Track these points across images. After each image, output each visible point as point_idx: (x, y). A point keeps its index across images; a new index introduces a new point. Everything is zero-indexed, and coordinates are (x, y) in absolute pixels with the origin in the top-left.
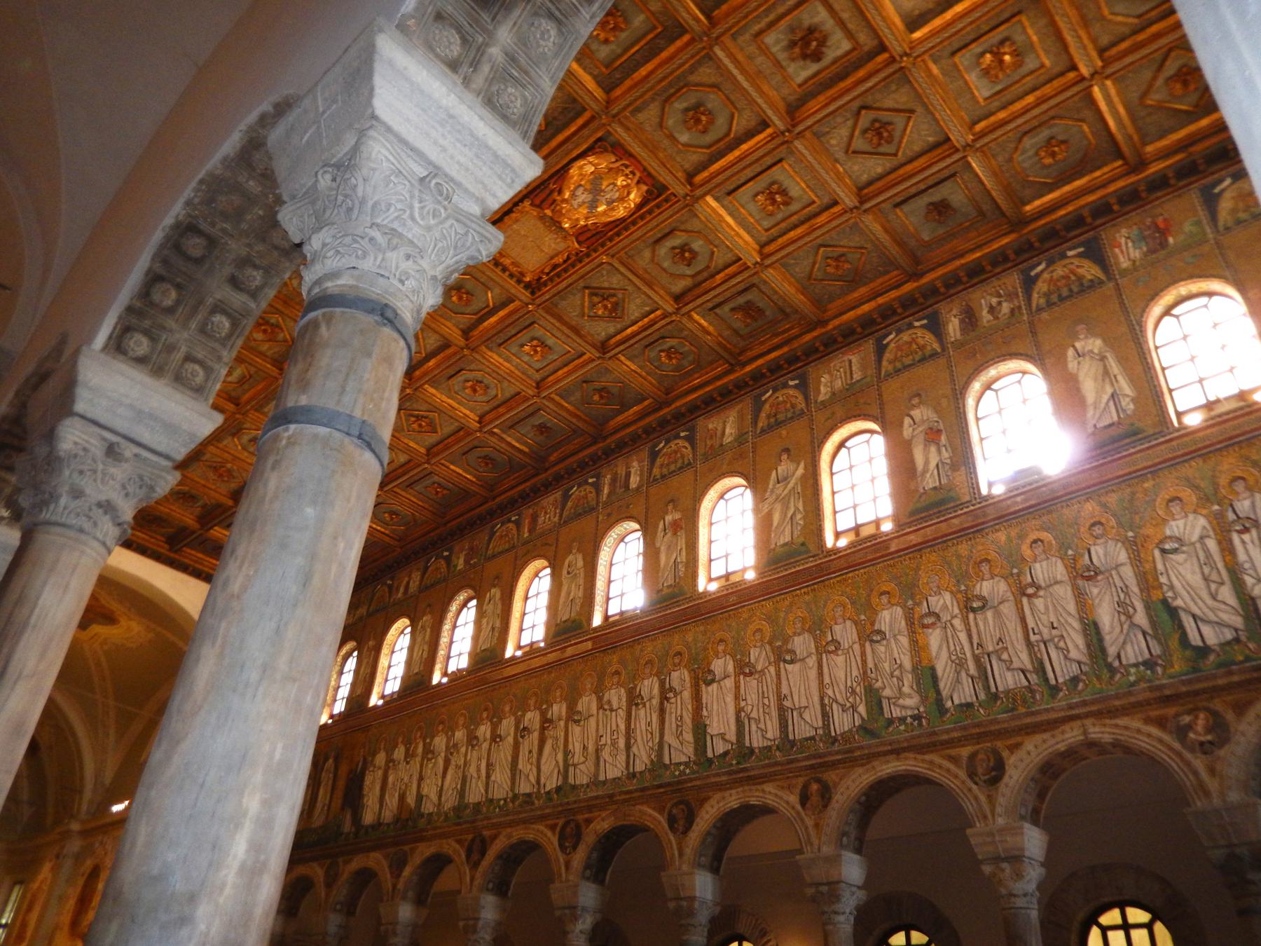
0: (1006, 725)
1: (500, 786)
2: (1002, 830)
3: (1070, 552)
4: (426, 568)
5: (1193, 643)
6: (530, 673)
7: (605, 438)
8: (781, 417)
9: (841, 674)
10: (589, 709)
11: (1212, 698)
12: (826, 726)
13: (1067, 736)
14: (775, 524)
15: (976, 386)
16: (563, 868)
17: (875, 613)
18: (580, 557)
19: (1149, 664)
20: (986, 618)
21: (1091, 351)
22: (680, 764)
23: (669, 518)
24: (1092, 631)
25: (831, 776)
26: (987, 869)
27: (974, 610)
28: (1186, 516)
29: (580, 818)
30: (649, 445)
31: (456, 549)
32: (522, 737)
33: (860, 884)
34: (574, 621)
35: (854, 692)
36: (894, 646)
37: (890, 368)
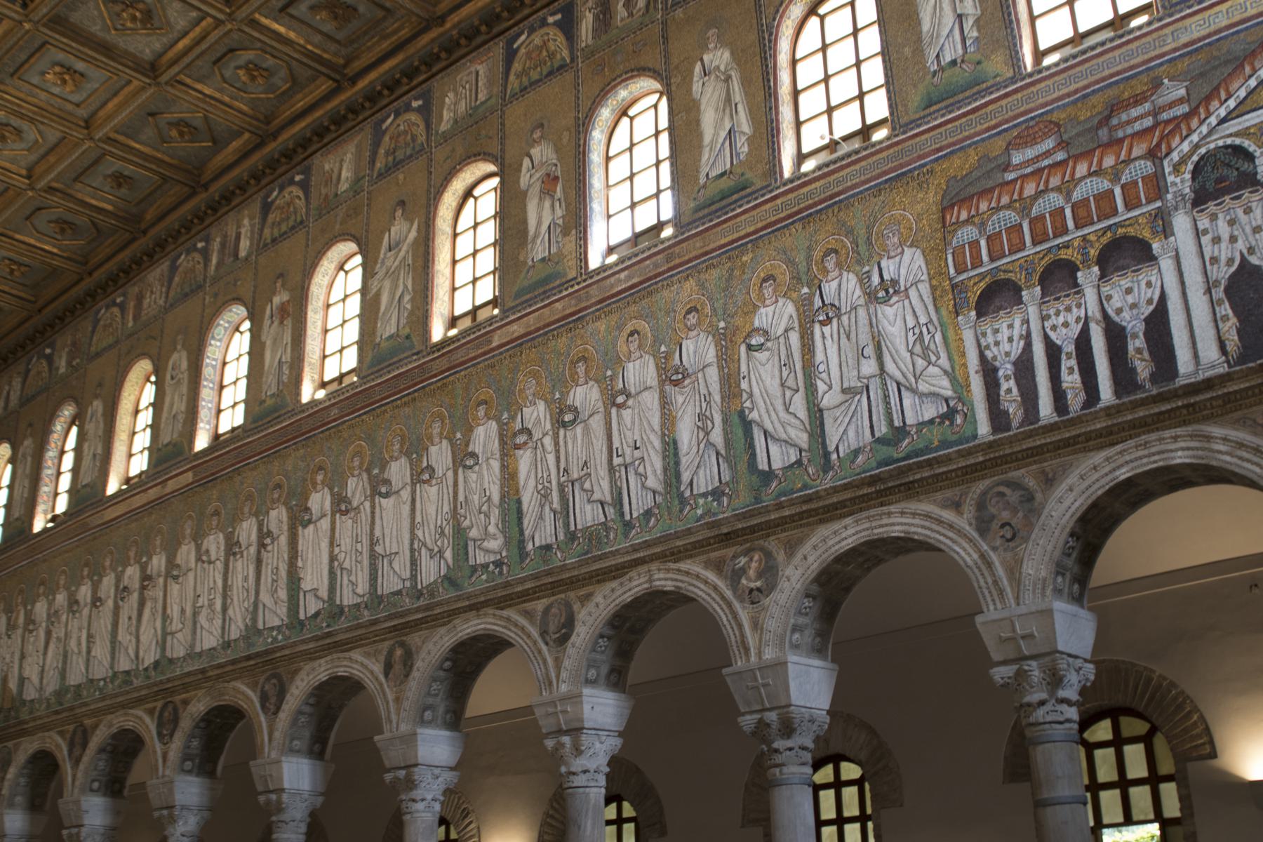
1: (100, 662)
2: (563, 699)
3: (663, 349)
4: (28, 371)
5: (760, 467)
6: (133, 515)
7: (206, 187)
8: (400, 155)
9: (431, 510)
10: (187, 562)
11: (768, 536)
12: (414, 577)
13: (635, 583)
14: (383, 308)
15: (605, 114)
16: (160, 761)
17: (470, 430)
18: (184, 354)
19: (717, 494)
21: (718, 68)
22: (272, 628)
23: (277, 300)
24: (671, 449)
25: (414, 639)
26: (550, 743)
27: (564, 425)
28: (777, 301)
29: (177, 698)
30: (262, 194)
31: (59, 344)
32: (122, 599)
33: (452, 763)
34: (175, 445)
35: (442, 533)
36: (485, 473)
37: (516, 86)
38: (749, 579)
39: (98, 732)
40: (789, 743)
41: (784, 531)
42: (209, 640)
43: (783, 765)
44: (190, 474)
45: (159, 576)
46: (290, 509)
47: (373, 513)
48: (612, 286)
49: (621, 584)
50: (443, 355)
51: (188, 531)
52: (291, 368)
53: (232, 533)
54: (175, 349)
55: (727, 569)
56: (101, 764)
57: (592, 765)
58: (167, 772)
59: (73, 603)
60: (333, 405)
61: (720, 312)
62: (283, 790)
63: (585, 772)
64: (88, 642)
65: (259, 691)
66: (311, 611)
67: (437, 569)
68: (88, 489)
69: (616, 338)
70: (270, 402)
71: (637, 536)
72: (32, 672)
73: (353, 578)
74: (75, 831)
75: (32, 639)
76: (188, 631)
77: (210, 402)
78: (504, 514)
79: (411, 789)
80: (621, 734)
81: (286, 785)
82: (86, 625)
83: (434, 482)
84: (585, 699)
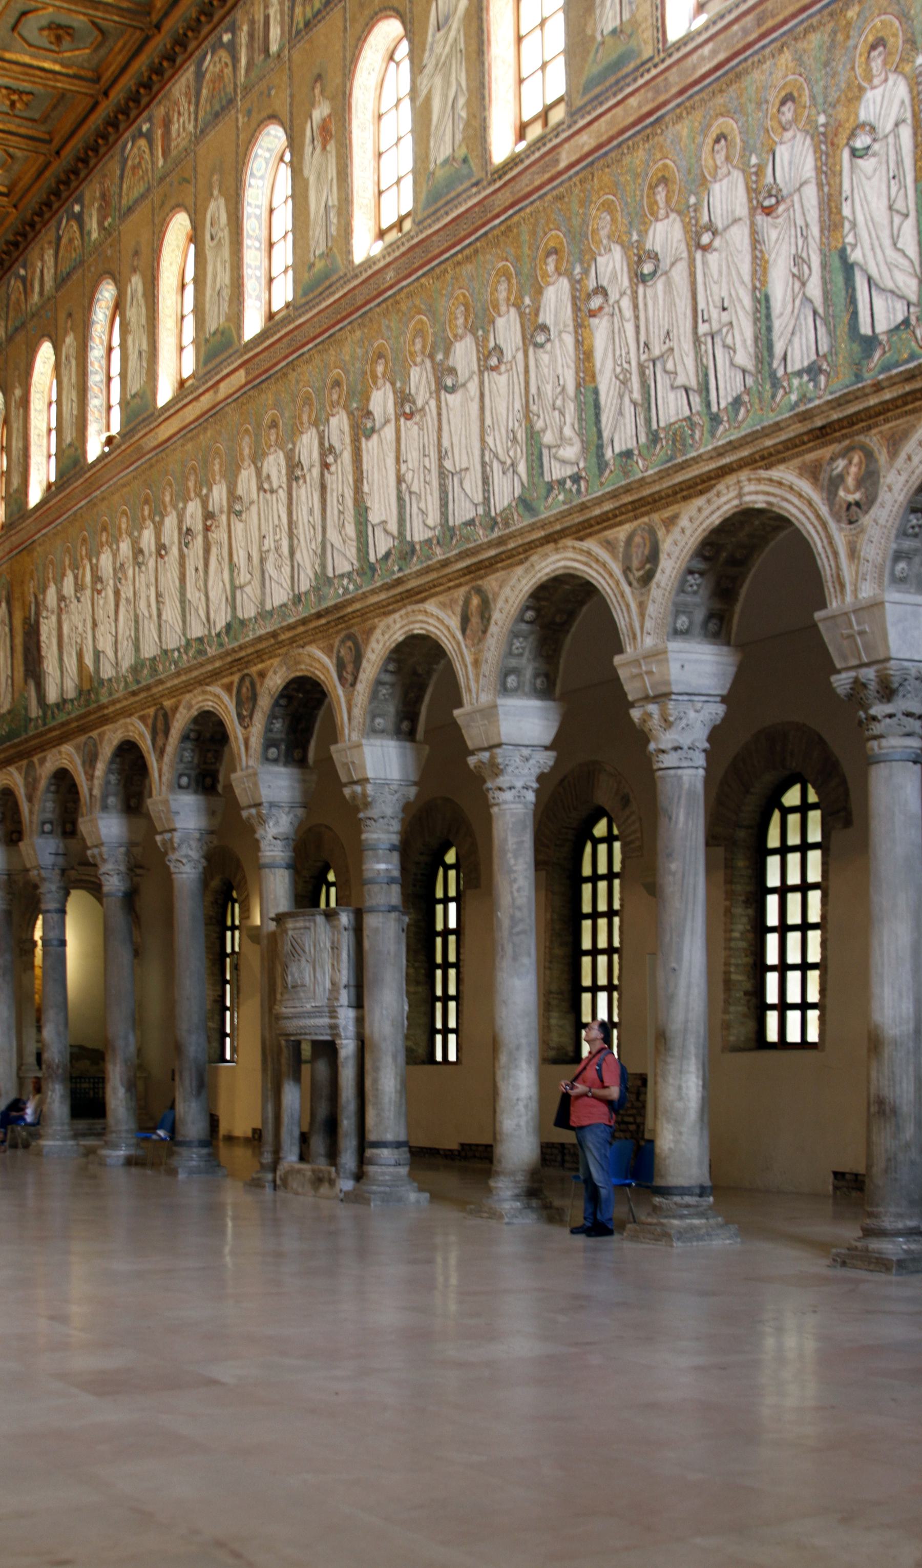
0: (657, 488)
3: (754, 160)
6: (187, 432)
9: (502, 409)
10: (249, 492)
11: (869, 428)
12: (486, 500)
13: (723, 499)
17: (539, 292)
18: (222, 201)
19: (813, 371)
20: (655, 296)
22: (342, 576)
25: (490, 583)
28: (886, 80)
29: (254, 670)
32: (187, 545)
34: (223, 333)
38: (848, 491)
39: (178, 715)
40: (888, 708)
41: (887, 421)
42: (279, 596)
43: (881, 736)
44: (242, 372)
45: (221, 512)
46: (350, 414)
47: (439, 415)
48: (694, 68)
49: (709, 501)
50: (505, 185)
51: (246, 451)
52: (339, 214)
53: (293, 450)
54: (212, 195)
55: (824, 476)
56: (187, 755)
57: (685, 740)
58: (251, 763)
59: (138, 552)
60: (388, 265)
61: (820, 100)
62: (367, 780)
63: (676, 749)
64: (158, 602)
65: (335, 655)
66: (382, 551)
67: (510, 489)
68: (137, 400)
69: (700, 146)
70: (320, 265)
71: (725, 435)
72: (105, 644)
73: (422, 506)
74: (167, 836)
75: (101, 602)
76: (256, 583)
77: (259, 268)
78: (580, 409)
79: (497, 775)
80: (724, 700)
81: (370, 774)
82: (153, 581)
83: (503, 368)
84: (671, 655)
